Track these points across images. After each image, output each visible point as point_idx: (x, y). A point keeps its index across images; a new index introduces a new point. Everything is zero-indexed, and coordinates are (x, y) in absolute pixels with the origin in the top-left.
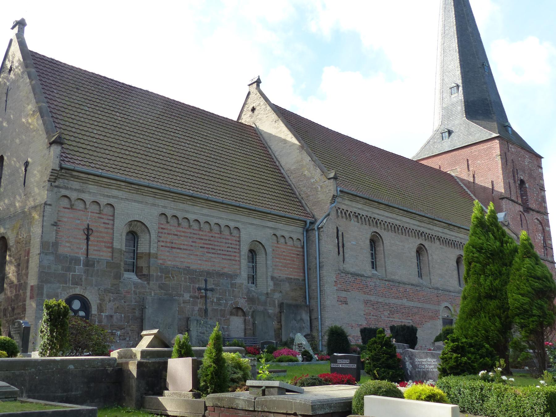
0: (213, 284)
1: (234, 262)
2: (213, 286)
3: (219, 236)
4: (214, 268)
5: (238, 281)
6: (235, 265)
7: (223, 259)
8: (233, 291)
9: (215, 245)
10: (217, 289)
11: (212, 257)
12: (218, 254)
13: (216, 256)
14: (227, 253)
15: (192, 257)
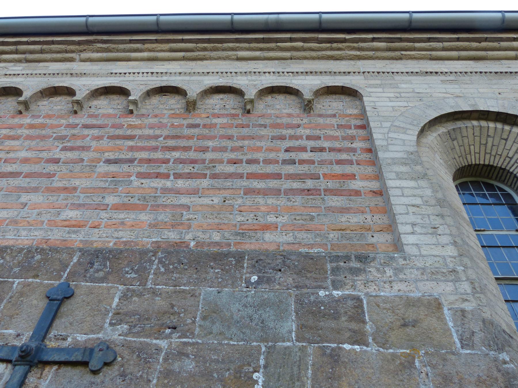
0: (119, 317)
1: (335, 201)
2: (114, 334)
3: (236, 122)
4: (172, 236)
5: (379, 287)
6: (344, 210)
7: (249, 191)
8: (335, 357)
9: (205, 150)
10: (145, 355)
11: (165, 190)
12: (214, 176)
13: (205, 183)
14: (290, 169)
15: (24, 198)
